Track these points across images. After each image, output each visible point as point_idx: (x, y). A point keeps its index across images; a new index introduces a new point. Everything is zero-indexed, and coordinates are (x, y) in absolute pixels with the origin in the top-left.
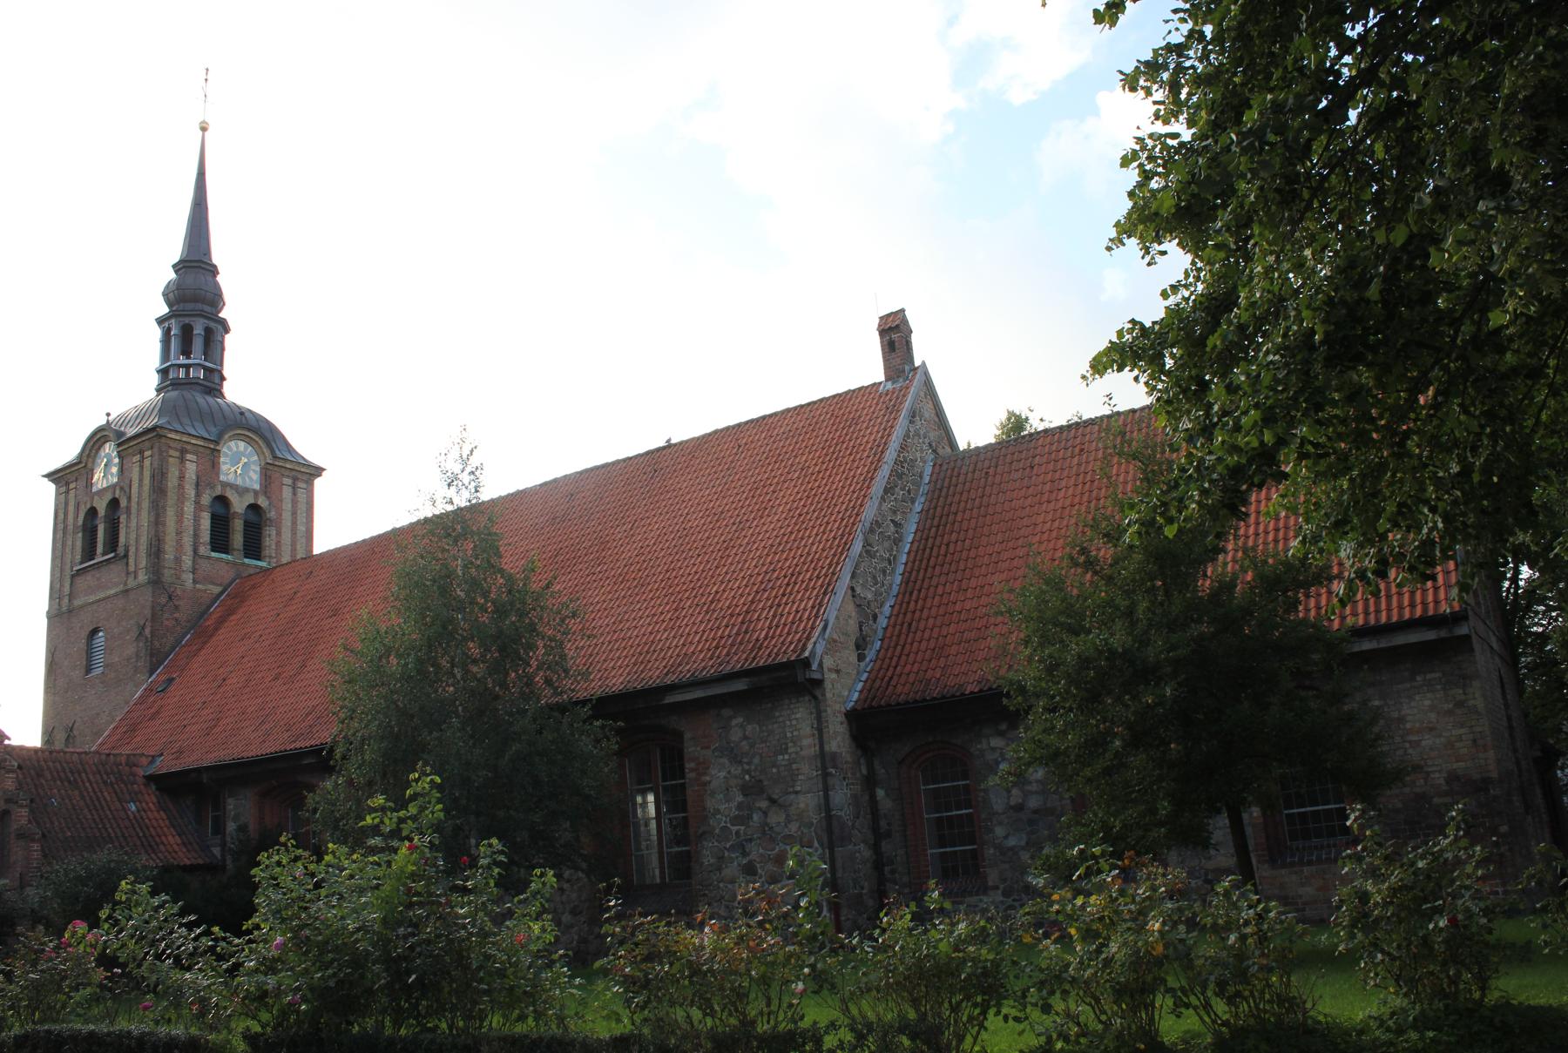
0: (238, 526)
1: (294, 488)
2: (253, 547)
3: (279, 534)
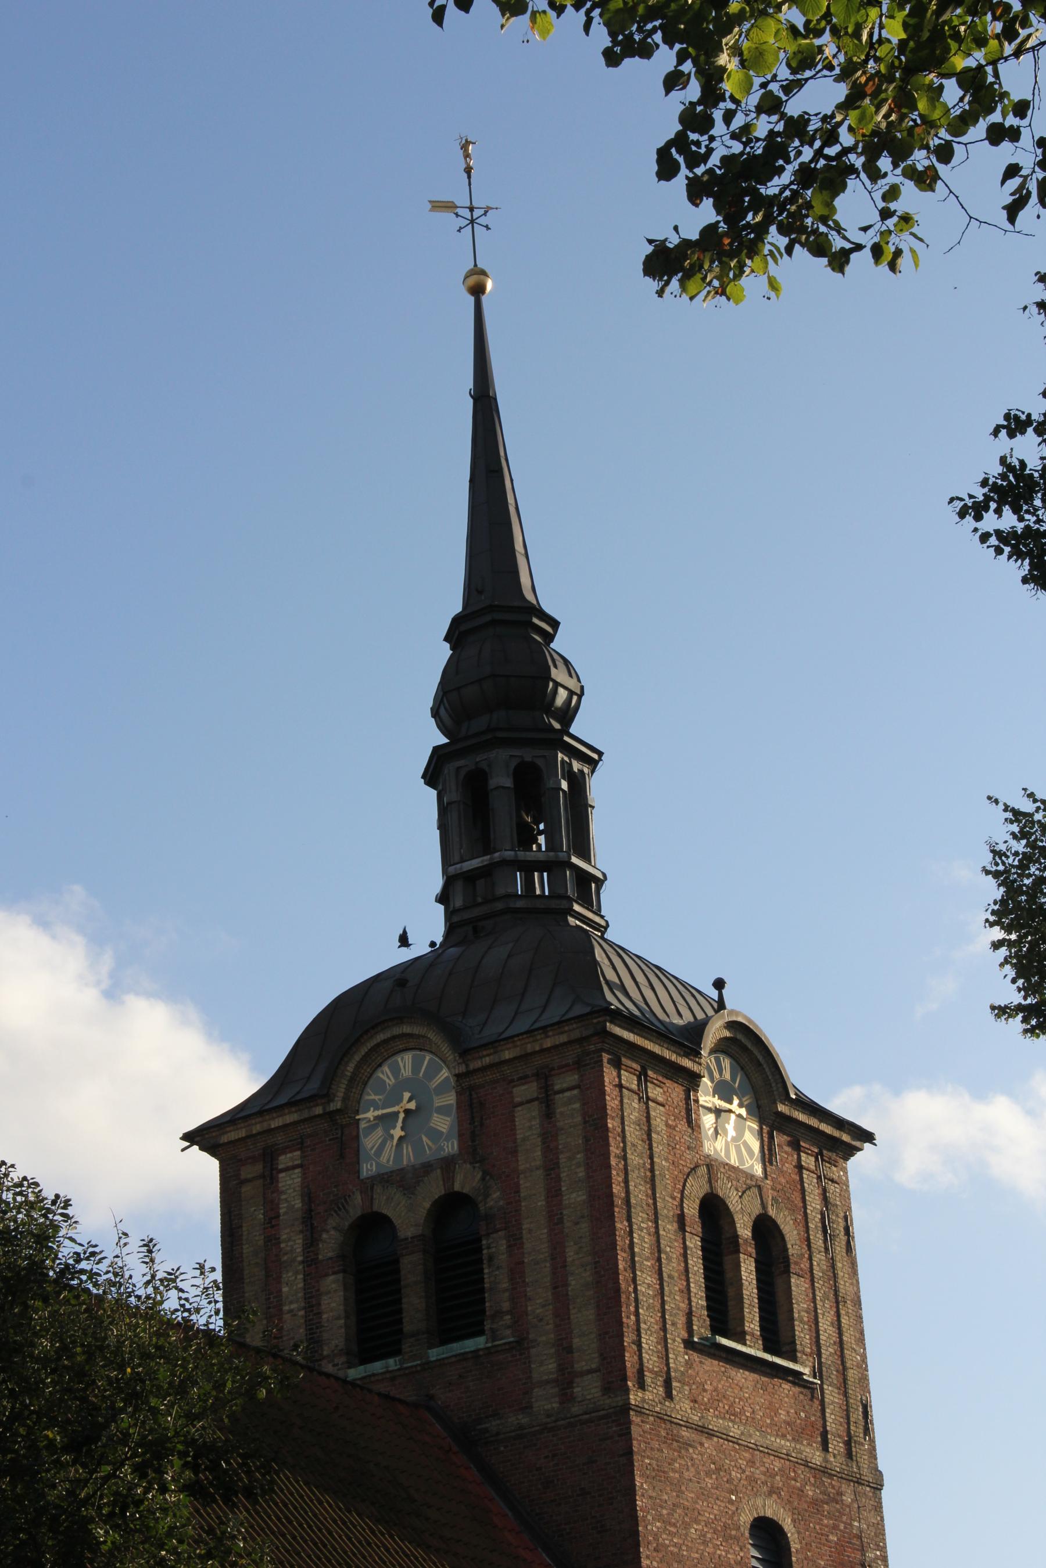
0: (412, 1269)
1: (547, 1102)
2: (460, 1305)
3: (515, 1242)
